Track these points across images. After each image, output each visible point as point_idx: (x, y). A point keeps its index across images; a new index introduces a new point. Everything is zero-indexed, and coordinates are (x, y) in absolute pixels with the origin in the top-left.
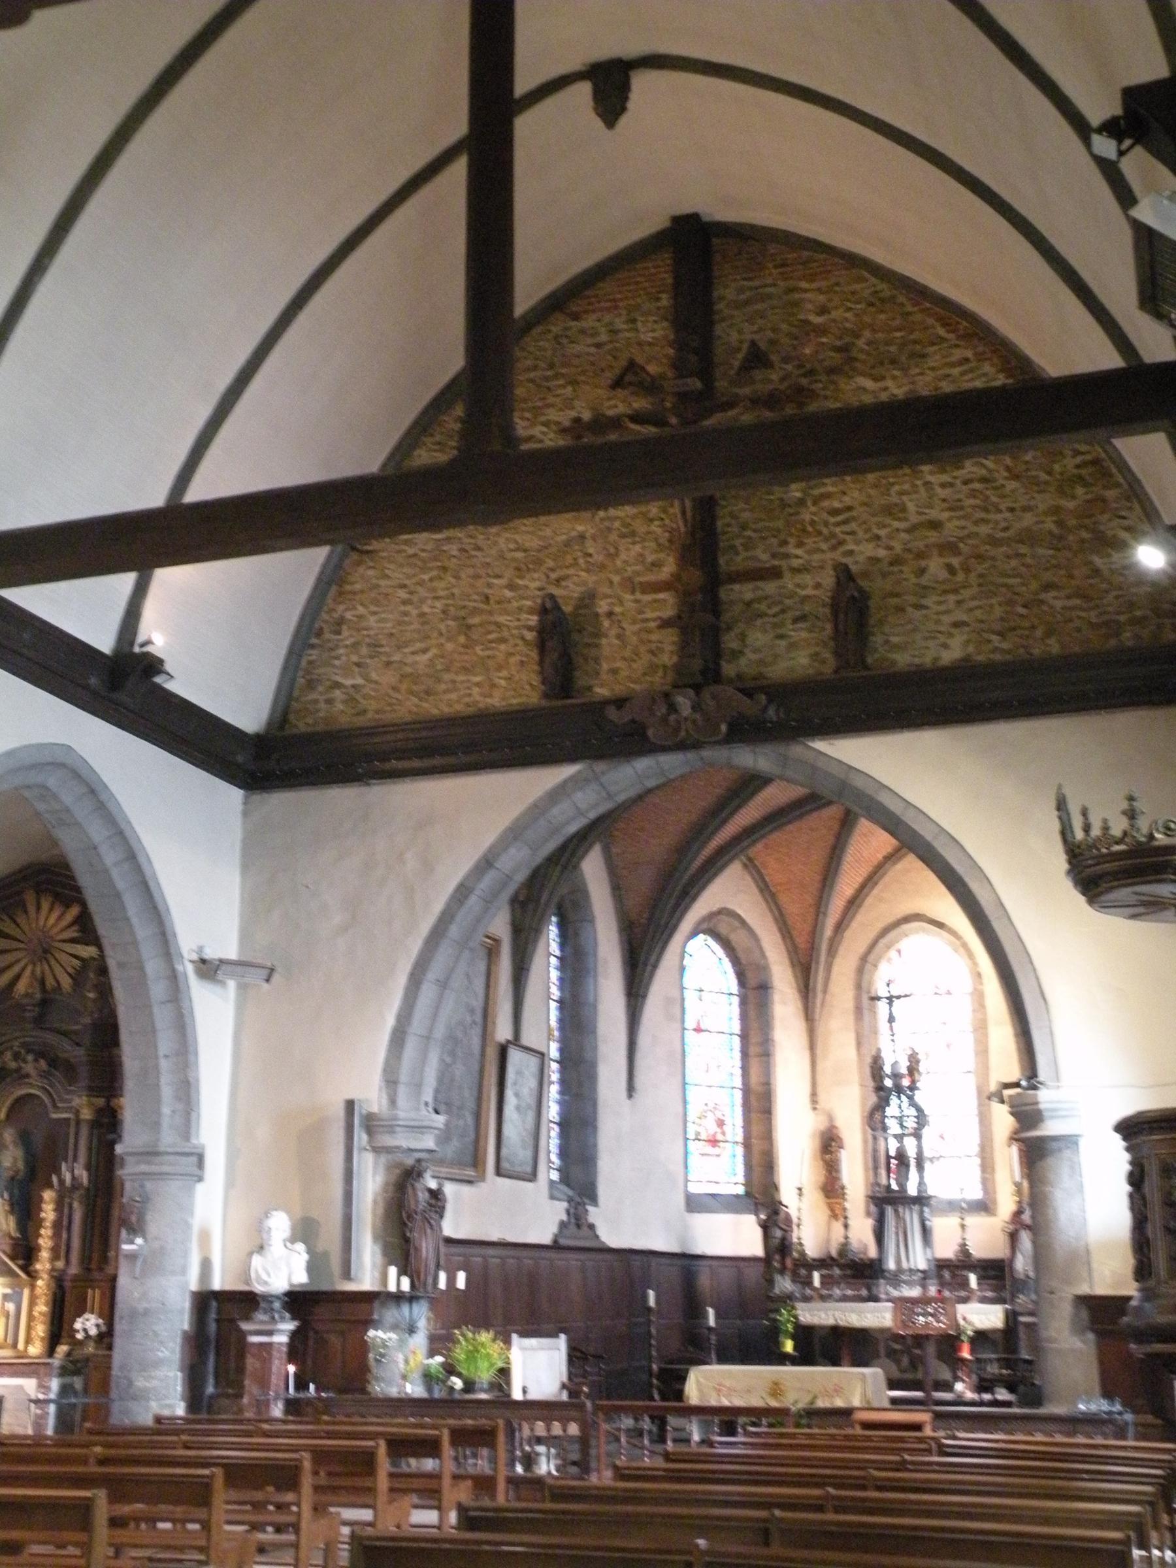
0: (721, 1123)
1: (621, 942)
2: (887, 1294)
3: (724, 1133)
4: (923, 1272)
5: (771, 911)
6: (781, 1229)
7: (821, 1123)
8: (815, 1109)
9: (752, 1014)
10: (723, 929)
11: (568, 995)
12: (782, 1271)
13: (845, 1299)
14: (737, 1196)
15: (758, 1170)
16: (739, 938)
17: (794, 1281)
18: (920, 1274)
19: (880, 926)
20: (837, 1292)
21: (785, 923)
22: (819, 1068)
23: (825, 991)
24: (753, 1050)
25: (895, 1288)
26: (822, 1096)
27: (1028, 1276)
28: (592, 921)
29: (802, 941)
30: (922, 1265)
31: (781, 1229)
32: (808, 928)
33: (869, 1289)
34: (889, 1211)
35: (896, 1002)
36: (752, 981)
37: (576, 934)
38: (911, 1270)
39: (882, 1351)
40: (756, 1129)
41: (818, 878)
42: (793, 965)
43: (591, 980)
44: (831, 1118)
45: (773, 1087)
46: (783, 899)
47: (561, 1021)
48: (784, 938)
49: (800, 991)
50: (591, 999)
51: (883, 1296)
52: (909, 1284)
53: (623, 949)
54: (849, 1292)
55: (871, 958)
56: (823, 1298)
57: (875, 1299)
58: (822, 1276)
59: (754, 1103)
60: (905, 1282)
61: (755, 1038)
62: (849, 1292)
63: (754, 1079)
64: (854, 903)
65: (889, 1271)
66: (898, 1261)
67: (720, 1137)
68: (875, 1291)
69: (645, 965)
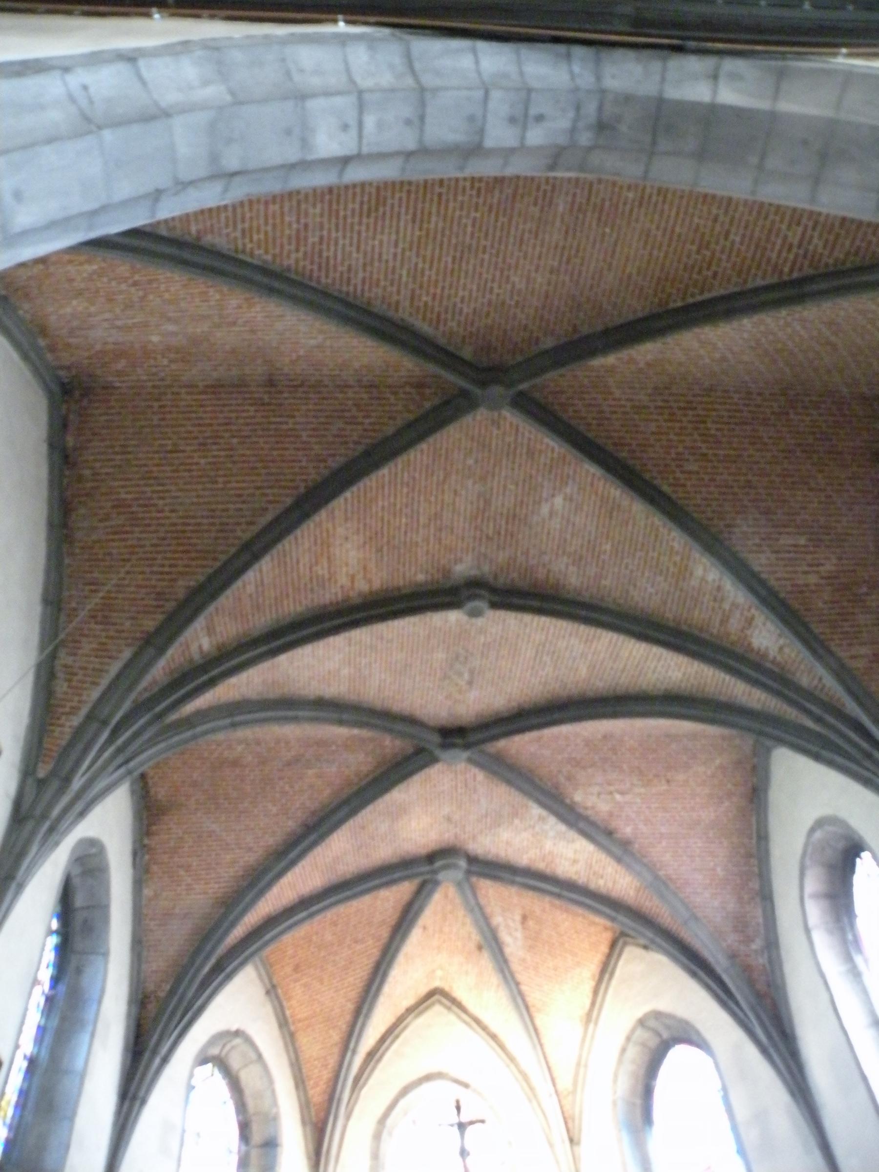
1: (129, 1015)
5: (287, 1051)
10: (235, 1062)
11: (44, 1054)
16: (249, 1077)
21: (300, 1070)
28: (106, 955)
29: (317, 1094)
32: (326, 1075)
35: (470, 1130)
36: (257, 1137)
37: (79, 971)
41: (350, 1007)
42: (304, 1123)
43: (85, 1038)
46: (303, 1040)
47: (23, 1094)
48: (297, 1087)
50: (79, 1063)
53: (128, 1027)
64: (373, 1056)
69: (155, 1052)
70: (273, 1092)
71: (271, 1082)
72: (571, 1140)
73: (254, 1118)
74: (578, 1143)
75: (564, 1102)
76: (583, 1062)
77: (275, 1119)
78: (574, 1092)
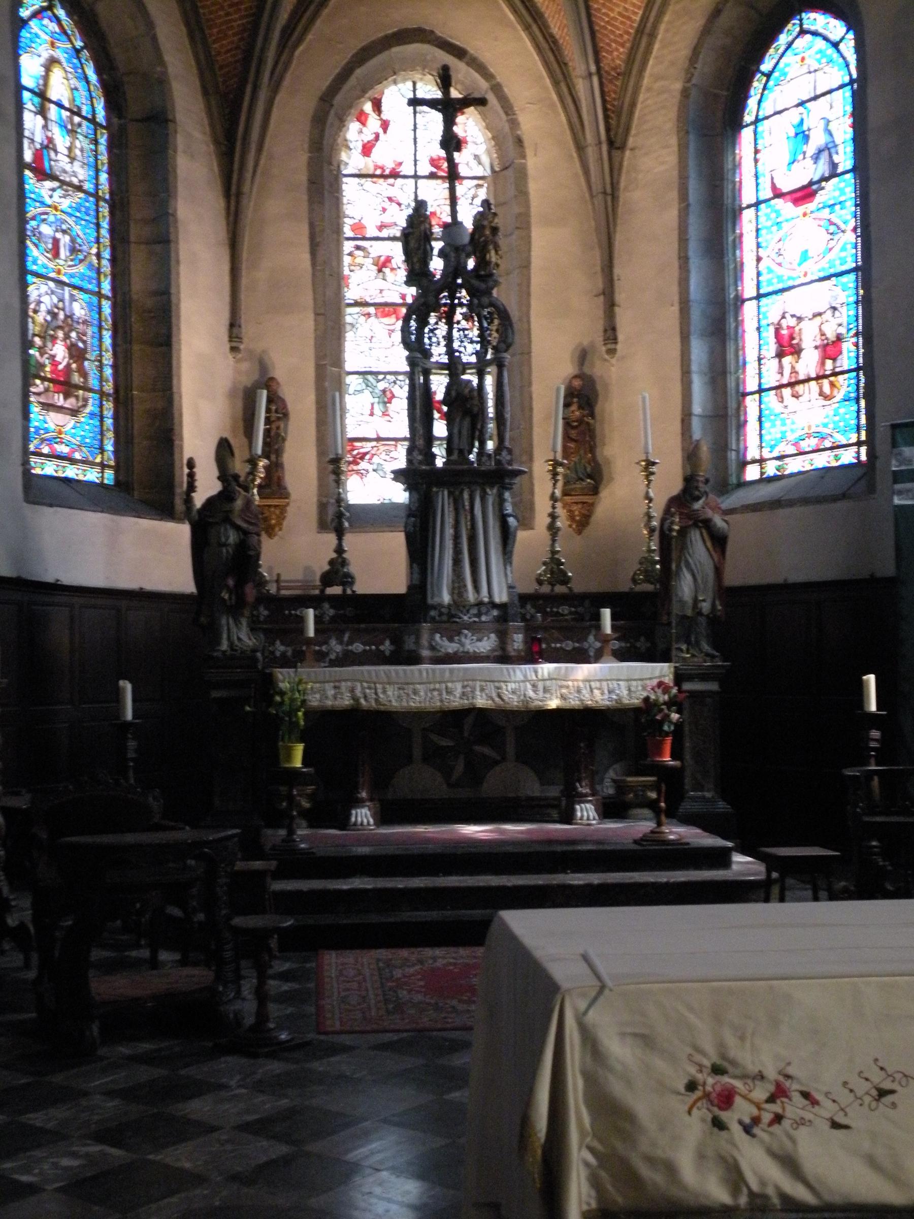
0: (77, 354)
2: (432, 648)
3: (84, 374)
4: (502, 607)
6: (238, 528)
7: (248, 374)
8: (234, 349)
9: (135, 167)
12: (235, 609)
13: (347, 660)
14: (102, 485)
15: (141, 446)
17: (253, 629)
18: (495, 613)
19: (356, 45)
20: (335, 647)
22: (244, 281)
23: (260, 149)
24: (135, 232)
25: (451, 640)
26: (248, 329)
27: (700, 614)
30: (501, 596)
31: (238, 528)
33: (397, 641)
34: (443, 499)
36: (134, 109)
38: (480, 604)
39: (417, 752)
40: (140, 372)
42: (205, 92)
44: (263, 366)
45: (174, 299)
49: (216, 142)
51: (425, 653)
52: (474, 628)
54: (358, 647)
55: (338, 99)
56: (321, 657)
57: (413, 659)
58: (318, 620)
59: (137, 326)
60: (469, 627)
61: (138, 211)
62: (358, 647)
63: (138, 285)
65: (438, 607)
66: (458, 588)
67: (76, 379)
68: (409, 643)
70: (154, 39)
71: (150, 25)
72: (611, 143)
73: (125, 79)
74: (622, 148)
75: (609, 87)
76: (647, 30)
77: (162, 82)
78: (627, 74)
